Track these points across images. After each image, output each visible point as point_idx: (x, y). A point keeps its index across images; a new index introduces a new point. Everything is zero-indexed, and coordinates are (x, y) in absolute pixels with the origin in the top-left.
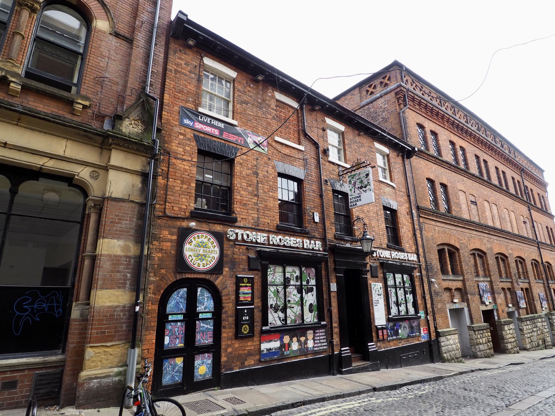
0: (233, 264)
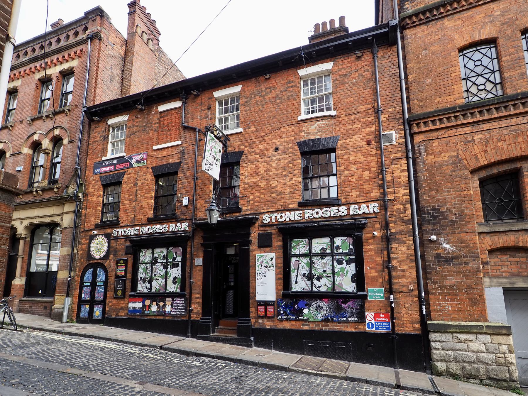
0: (116, 252)
